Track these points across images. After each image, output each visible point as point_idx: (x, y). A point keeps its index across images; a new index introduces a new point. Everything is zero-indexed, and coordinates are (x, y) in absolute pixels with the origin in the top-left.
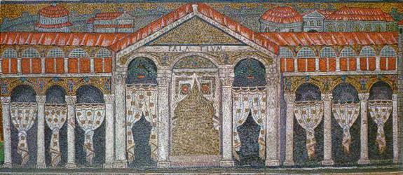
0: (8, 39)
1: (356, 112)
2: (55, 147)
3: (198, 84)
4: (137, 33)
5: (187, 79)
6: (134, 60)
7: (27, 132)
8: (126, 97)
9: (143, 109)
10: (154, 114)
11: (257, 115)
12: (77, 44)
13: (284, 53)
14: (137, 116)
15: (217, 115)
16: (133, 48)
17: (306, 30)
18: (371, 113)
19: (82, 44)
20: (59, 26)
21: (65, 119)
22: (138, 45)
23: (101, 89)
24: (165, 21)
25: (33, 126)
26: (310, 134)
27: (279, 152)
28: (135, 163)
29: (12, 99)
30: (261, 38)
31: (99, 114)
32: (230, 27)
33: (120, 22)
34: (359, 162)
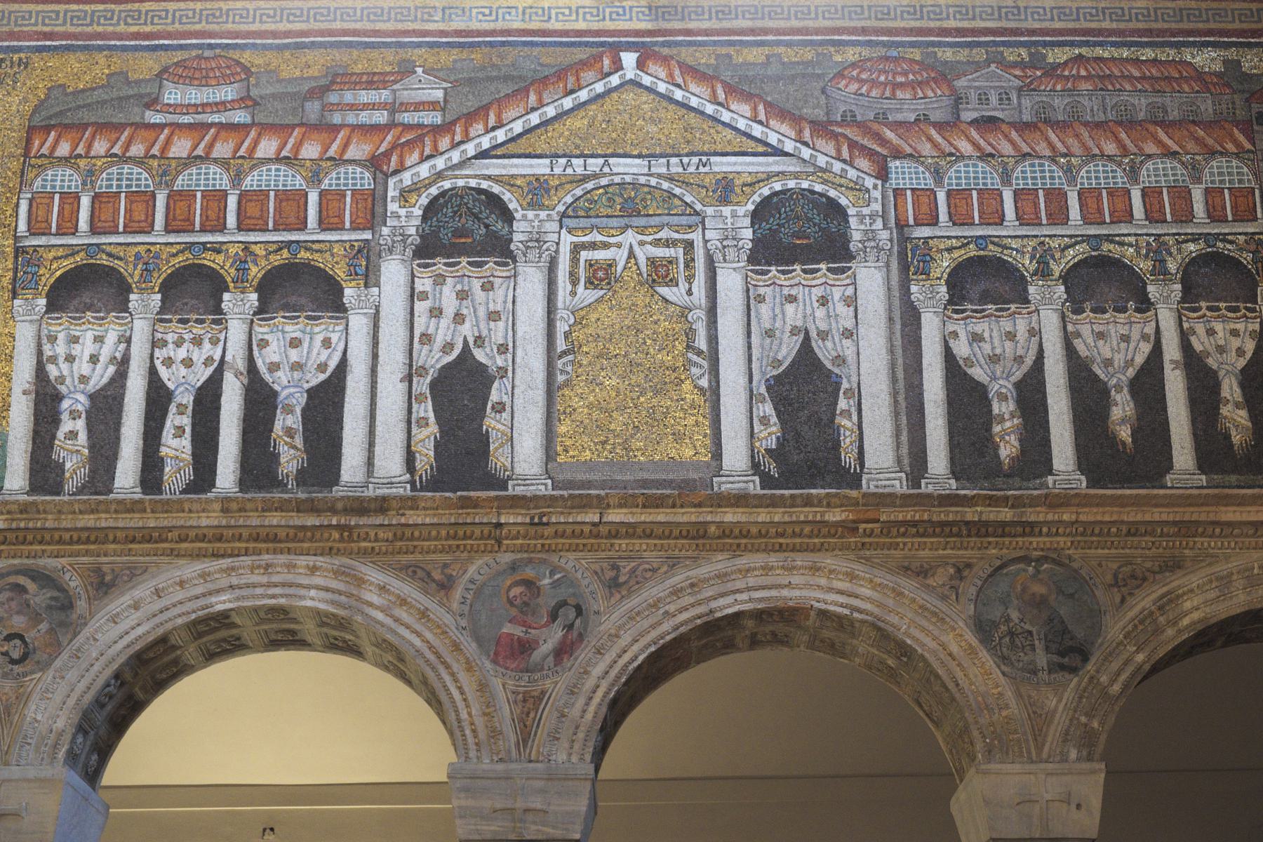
0: (57, 142)
1: (1145, 337)
2: (177, 446)
4: (453, 123)
5: (606, 246)
6: (443, 194)
7: (92, 397)
8: (412, 295)
9: (467, 330)
11: (829, 344)
12: (271, 153)
13: (903, 174)
15: (701, 343)
16: (440, 163)
18: (1193, 339)
19: (284, 153)
20: (221, 106)
21: (217, 357)
22: (456, 156)
23: (340, 273)
25: (113, 380)
26: (1003, 398)
27: (905, 450)
28: (435, 483)
29: (52, 307)
30: (835, 136)
31: (327, 343)
32: (733, 107)
33: (405, 96)
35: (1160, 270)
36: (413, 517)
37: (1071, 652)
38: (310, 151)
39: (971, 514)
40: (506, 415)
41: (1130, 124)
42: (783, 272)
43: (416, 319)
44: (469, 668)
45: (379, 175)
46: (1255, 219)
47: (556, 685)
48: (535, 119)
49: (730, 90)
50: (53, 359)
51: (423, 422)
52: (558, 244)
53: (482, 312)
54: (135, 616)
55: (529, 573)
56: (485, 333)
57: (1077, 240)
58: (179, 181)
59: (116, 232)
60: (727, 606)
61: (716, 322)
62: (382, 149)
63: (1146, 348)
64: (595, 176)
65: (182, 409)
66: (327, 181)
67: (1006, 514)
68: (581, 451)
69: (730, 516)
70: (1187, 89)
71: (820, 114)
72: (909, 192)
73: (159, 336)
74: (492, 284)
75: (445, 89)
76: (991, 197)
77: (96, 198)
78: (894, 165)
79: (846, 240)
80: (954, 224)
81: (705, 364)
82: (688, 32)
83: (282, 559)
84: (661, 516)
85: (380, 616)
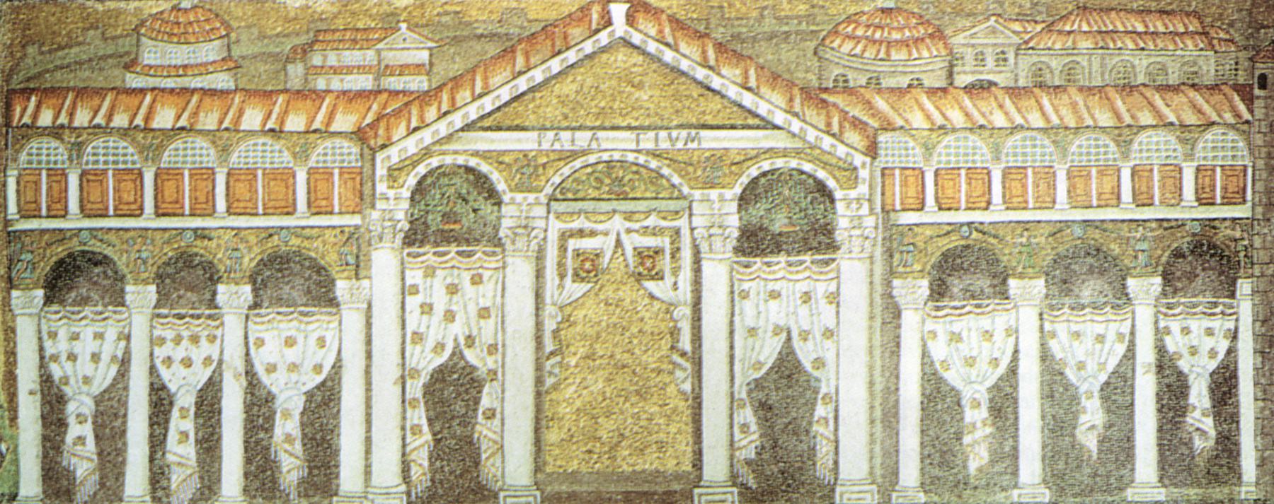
0: (38, 107)
1: (1121, 336)
2: (182, 450)
4: (440, 88)
5: (593, 233)
6: (431, 173)
7: (98, 401)
10: (491, 342)
11: (810, 344)
12: (256, 126)
14: (440, 347)
15: (686, 343)
16: (427, 136)
17: (962, 80)
19: (269, 125)
20: (203, 68)
21: (216, 357)
22: (442, 128)
24: (527, 56)
27: (878, 461)
29: (48, 300)
31: (322, 342)
32: (724, 72)
40: (497, 422)
42: (768, 264)
43: (407, 316)
45: (366, 150)
46: (1244, 202)
48: (522, 84)
50: (55, 358)
51: (416, 430)
52: (546, 231)
53: (472, 309)
56: (475, 333)
58: (165, 157)
61: (699, 319)
62: (368, 120)
63: (1121, 349)
64: (584, 153)
65: (184, 413)
66: (314, 158)
68: (569, 461)
70: (1191, 47)
72: (897, 172)
73: (156, 333)
74: (480, 276)
75: (430, 49)
76: (980, 175)
77: (83, 174)
80: (940, 209)
81: (688, 365)
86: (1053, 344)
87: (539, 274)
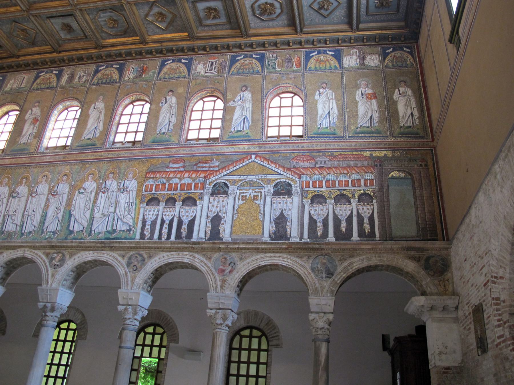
1: (349, 210)
2: (165, 231)
3: (252, 196)
5: (246, 193)
13: (304, 178)
14: (215, 212)
15: (262, 212)
16: (217, 177)
20: (179, 167)
22: (220, 176)
23: (196, 198)
26: (320, 222)
27: (299, 233)
28: (209, 239)
29: (147, 205)
30: (291, 170)
31: (193, 212)
33: (212, 165)
34: (352, 239)
35: (354, 196)
36: (204, 246)
37: (330, 274)
38: (194, 175)
39: (310, 246)
41: (349, 167)
44: (213, 275)
47: (229, 278)
48: (235, 168)
49: (272, 162)
50: (146, 215)
51: (209, 227)
53: (221, 206)
54: (155, 263)
55: (226, 256)
57: (337, 190)
59: (159, 191)
60: (262, 264)
63: (350, 212)
67: (317, 246)
69: (263, 246)
71: (289, 167)
76: (321, 182)
77: (156, 185)
78: (302, 176)
79: (291, 191)
82: (265, 151)
83: (181, 253)
84: (251, 246)
85: (198, 264)
86: (336, 211)
87: (235, 200)
